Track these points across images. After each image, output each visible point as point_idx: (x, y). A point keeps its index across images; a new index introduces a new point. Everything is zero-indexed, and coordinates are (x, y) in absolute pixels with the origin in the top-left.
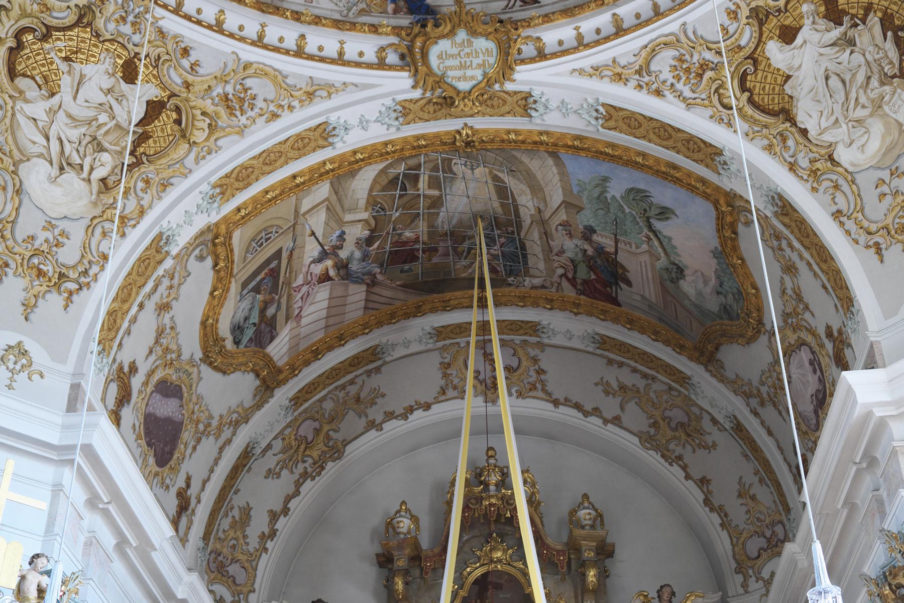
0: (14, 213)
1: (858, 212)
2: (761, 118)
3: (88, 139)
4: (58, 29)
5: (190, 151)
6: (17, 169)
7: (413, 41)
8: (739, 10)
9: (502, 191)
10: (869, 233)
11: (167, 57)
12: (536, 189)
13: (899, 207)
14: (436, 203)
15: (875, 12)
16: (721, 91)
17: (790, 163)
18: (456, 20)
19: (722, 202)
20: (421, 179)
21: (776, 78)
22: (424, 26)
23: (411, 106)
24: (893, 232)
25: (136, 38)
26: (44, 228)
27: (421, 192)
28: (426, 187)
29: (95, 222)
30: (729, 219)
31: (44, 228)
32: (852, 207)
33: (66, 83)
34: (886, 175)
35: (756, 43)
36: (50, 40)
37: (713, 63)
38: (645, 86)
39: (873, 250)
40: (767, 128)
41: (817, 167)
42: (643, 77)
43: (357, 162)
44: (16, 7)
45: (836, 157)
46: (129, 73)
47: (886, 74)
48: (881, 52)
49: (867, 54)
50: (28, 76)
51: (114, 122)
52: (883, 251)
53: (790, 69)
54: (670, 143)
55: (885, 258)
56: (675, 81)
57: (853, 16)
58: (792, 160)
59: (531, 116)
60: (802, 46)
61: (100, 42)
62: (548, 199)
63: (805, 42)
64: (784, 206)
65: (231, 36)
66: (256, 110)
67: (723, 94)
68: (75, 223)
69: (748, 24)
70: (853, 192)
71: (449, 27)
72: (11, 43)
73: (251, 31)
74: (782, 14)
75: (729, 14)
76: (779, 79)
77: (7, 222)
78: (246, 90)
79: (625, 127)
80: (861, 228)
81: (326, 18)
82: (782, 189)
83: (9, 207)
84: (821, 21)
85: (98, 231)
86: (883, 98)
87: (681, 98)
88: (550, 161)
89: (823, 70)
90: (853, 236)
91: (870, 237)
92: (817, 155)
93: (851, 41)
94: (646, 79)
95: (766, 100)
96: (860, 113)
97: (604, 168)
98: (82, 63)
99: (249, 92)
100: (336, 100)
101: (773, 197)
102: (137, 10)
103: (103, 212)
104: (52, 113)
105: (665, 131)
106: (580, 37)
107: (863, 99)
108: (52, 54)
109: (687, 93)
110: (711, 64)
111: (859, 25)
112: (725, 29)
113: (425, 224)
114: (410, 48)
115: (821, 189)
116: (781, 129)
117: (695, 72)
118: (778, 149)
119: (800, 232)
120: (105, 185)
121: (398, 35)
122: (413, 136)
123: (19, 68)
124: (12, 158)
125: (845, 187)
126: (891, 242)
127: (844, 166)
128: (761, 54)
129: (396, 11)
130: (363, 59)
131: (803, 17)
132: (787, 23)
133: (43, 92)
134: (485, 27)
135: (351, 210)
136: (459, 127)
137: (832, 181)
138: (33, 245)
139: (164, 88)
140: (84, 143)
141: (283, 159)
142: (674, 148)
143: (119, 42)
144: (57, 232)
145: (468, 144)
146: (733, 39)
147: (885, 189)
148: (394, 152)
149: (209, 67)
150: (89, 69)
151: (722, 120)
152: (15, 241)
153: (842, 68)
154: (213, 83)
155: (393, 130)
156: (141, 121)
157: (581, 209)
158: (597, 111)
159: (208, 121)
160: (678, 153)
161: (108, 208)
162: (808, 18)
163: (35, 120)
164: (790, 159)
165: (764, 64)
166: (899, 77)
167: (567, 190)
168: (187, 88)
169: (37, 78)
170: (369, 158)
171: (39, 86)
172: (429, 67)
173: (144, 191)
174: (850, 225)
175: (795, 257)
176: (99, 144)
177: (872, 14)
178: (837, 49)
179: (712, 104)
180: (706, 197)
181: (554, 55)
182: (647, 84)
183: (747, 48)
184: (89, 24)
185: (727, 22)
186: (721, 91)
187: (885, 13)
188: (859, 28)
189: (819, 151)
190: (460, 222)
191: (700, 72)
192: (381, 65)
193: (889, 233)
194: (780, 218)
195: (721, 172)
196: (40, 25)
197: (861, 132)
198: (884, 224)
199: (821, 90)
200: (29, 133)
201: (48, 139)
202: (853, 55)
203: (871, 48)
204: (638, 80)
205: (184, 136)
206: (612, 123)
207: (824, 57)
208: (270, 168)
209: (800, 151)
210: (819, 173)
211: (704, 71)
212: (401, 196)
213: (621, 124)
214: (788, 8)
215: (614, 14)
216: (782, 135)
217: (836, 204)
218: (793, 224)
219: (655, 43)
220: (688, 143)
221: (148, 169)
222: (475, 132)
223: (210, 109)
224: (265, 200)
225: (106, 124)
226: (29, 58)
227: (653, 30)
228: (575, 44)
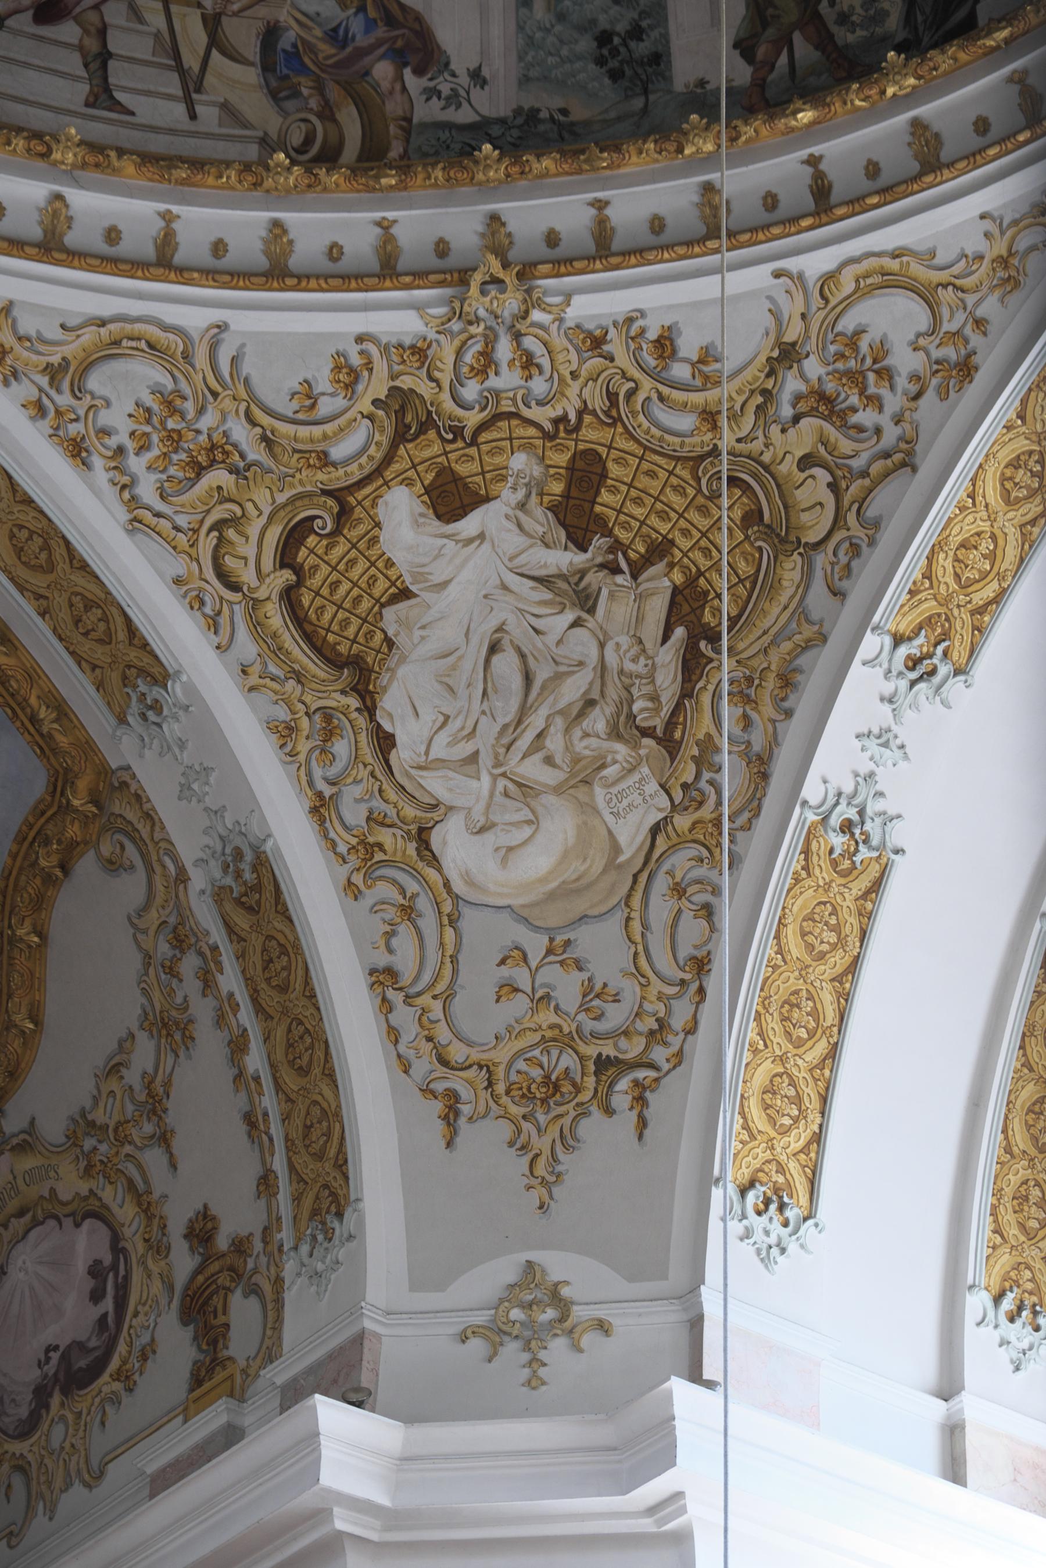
1: (435, 997)
2: (296, 652)
8: (366, 373)
10: (444, 1062)
13: (537, 1036)
15: (671, 566)
16: (231, 533)
17: (320, 795)
19: (83, 784)
21: (374, 579)
24: (500, 1088)
30: (74, 831)
32: (427, 978)
34: (536, 945)
35: (367, 471)
37: (242, 456)
38: (52, 413)
39: (438, 1106)
40: (299, 682)
41: (380, 839)
42: (59, 391)
45: (435, 839)
47: (631, 717)
48: (642, 661)
52: (462, 1121)
53: (419, 577)
54: (39, 581)
55: (458, 1140)
56: (130, 446)
57: (617, 546)
58: (328, 791)
60: (469, 541)
63: (481, 537)
64: (258, 887)
67: (231, 543)
69: (370, 417)
70: (442, 944)
74: (460, 444)
75: (337, 368)
76: (382, 584)
80: (429, 1039)
82: (277, 848)
84: (539, 512)
86: (603, 766)
87: (126, 495)
89: (493, 623)
90: (402, 1048)
91: (440, 1071)
92: (392, 812)
93: (588, 597)
94: (64, 399)
95: (327, 616)
96: (533, 770)
101: (238, 854)
105: (46, 547)
107: (555, 743)
109: (147, 490)
110: (237, 457)
111: (620, 571)
112: (309, 395)
115: (370, 897)
116: (334, 704)
117: (189, 451)
118: (304, 747)
119: (265, 969)
125: (428, 923)
126: (488, 1109)
127: (446, 871)
128: (367, 503)
131: (503, 478)
132: (462, 469)
137: (403, 891)
142: (39, 597)
146: (317, 431)
147: (522, 977)
151: (202, 603)
153: (540, 645)
160: (42, 615)
162: (514, 489)
164: (321, 786)
165: (361, 529)
166: (659, 741)
174: (404, 1016)
175: (203, 1010)
177: (660, 567)
178: (548, 596)
179: (193, 552)
182: (59, 413)
183: (341, 472)
185: (323, 384)
186: (231, 533)
187: (691, 581)
188: (619, 579)
189: (401, 804)
191: (202, 459)
193: (490, 1084)
194: (228, 906)
195: (130, 719)
198: (485, 1056)
199: (467, 665)
202: (577, 631)
203: (624, 640)
204: (41, 390)
207: (509, 598)
209: (356, 782)
210: (379, 856)
211: (213, 462)
214: (481, 439)
215: (59, 197)
216: (328, 718)
217: (390, 951)
218: (256, 941)
219: (128, 327)
220: (87, 608)
227: (140, 296)
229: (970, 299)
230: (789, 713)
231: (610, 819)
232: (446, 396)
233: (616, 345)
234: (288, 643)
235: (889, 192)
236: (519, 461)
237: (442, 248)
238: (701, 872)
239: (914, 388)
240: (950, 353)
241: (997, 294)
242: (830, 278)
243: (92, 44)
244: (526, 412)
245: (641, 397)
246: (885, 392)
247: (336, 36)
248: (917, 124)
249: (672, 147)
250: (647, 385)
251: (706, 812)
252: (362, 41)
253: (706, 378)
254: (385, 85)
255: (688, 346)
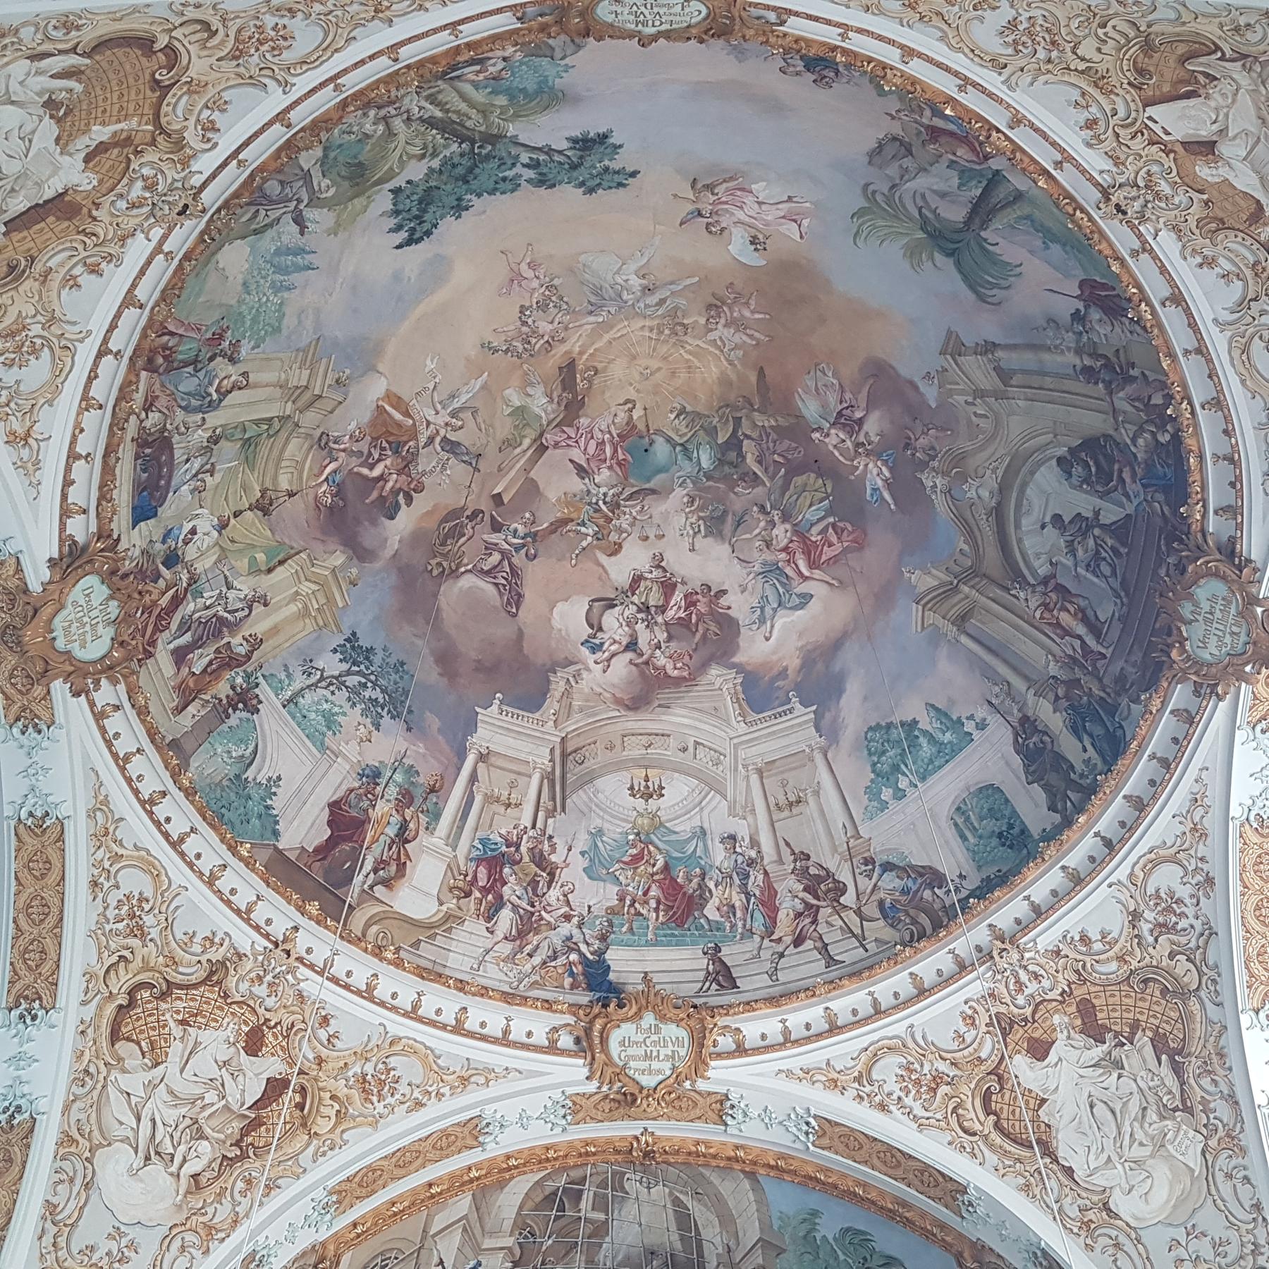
0: (76, 1214)
3: (188, 1122)
4: (180, 987)
5: (308, 1145)
6: (93, 1156)
7: (591, 1022)
9: (684, 1220)
11: (302, 1026)
12: (727, 1220)
14: (601, 1230)
18: (644, 1002)
19: (966, 1255)
20: (585, 1196)
22: (605, 1006)
23: (583, 1102)
25: (270, 1002)
26: (110, 1237)
27: (582, 1214)
28: (589, 1208)
29: (174, 1232)
31: (110, 1237)
33: (176, 1050)
34: (1180, 1235)
36: (169, 999)
43: (509, 1169)
44: (139, 959)
46: (253, 1044)
47: (1164, 1106)
49: (1139, 1079)
50: (133, 1041)
51: (223, 1102)
53: (1045, 1091)
54: (899, 1173)
56: (902, 1095)
59: (726, 1125)
60: (1056, 1064)
61: (227, 1004)
62: (741, 1234)
63: (1060, 1059)
65: (382, 1004)
66: (397, 1096)
68: (149, 1231)
69: (988, 1032)
71: (634, 1009)
72: (122, 1000)
73: (405, 1002)
75: (964, 1019)
76: (1032, 1101)
77: (65, 1225)
78: (388, 1071)
79: (842, 1148)
81: (493, 990)
83: (72, 1205)
84: (1077, 1036)
85: (177, 1243)
88: (746, 1184)
92: (1088, 1202)
94: (868, 1089)
96: (1137, 1152)
97: (814, 1200)
98: (200, 1028)
99: (392, 1073)
100: (495, 1089)
101: (1035, 1253)
102: (278, 970)
103: (187, 1219)
104: (151, 1086)
105: (893, 1156)
106: (786, 1032)
107: (1139, 1135)
108: (168, 1016)
109: (919, 1111)
111: (1124, 1044)
112: (960, 1036)
113: (583, 1258)
114: (588, 1031)
115: (1098, 1249)
118: (1037, 1191)
120: (196, 1182)
121: (574, 1015)
122: (581, 1140)
123: (124, 1030)
124: (90, 1140)
125: (1129, 1246)
129: (573, 987)
130: (531, 1041)
133: (146, 1060)
134: (677, 1011)
135: (492, 1234)
136: (638, 1133)
138: (90, 1258)
139: (291, 1064)
140: (181, 1127)
141: (420, 1161)
143: (249, 1006)
144: (124, 1242)
145: (647, 1154)
146: (971, 1049)
148: (555, 1159)
149: (349, 1041)
150: (206, 1036)
152: (69, 1252)
154: (350, 1060)
155: (558, 1130)
156: (256, 1103)
157: (785, 1251)
158: (808, 1124)
159: (337, 1107)
161: (194, 1214)
163: (128, 1094)
167: (765, 1225)
168: (319, 1064)
169: (143, 1044)
170: (524, 1165)
171: (143, 1054)
172: (608, 1055)
173: (243, 1193)
176: (200, 1129)
180: (946, 1246)
181: (757, 1051)
184: (219, 983)
185: (963, 1029)
186: (960, 1111)
190: (628, 1258)
191: (933, 1085)
192: (551, 1048)
196: (161, 981)
197: (1142, 1177)
200: (118, 1108)
201: (139, 1120)
203: (1143, 1073)
205: (304, 1125)
206: (825, 1142)
207: (1086, 1080)
208: (403, 1171)
210: (1093, 1226)
212: (557, 1218)
213: (836, 1142)
215: (827, 1008)
221: (252, 1165)
222: (657, 1140)
223: (342, 1092)
224: (390, 1213)
225: (213, 1104)
226: (138, 1019)
227: (874, 1031)
228: (781, 1039)
229: (1192, 852)
230: (1230, 1069)
231: (1180, 1158)
232: (1012, 1007)
233: (1065, 950)
234: (1008, 1148)
235: (1132, 830)
236: (1057, 1019)
237: (979, 949)
238: (1234, 1162)
239: (1194, 901)
240: (1199, 878)
241: (1201, 843)
242: (1131, 874)
243: (819, 944)
244: (1047, 997)
245: (1088, 965)
246: (1184, 909)
247: (905, 891)
248: (1125, 797)
249: (1039, 860)
250: (1087, 959)
251: (1221, 1133)
252: (914, 888)
253: (1109, 943)
254: (930, 899)
255: (1094, 935)
